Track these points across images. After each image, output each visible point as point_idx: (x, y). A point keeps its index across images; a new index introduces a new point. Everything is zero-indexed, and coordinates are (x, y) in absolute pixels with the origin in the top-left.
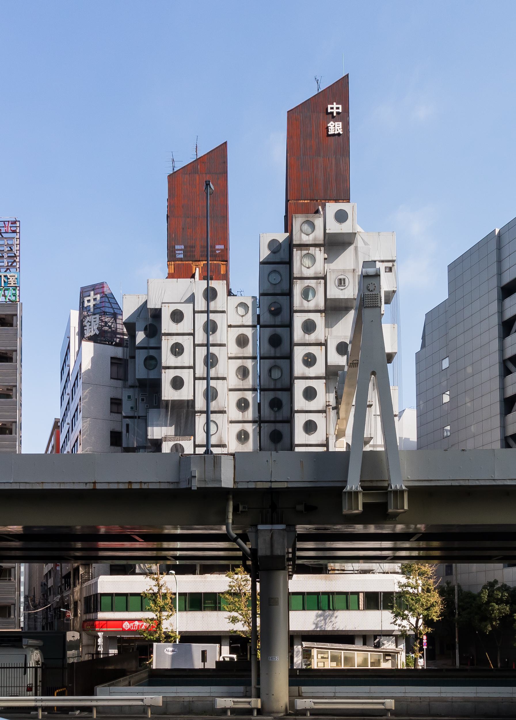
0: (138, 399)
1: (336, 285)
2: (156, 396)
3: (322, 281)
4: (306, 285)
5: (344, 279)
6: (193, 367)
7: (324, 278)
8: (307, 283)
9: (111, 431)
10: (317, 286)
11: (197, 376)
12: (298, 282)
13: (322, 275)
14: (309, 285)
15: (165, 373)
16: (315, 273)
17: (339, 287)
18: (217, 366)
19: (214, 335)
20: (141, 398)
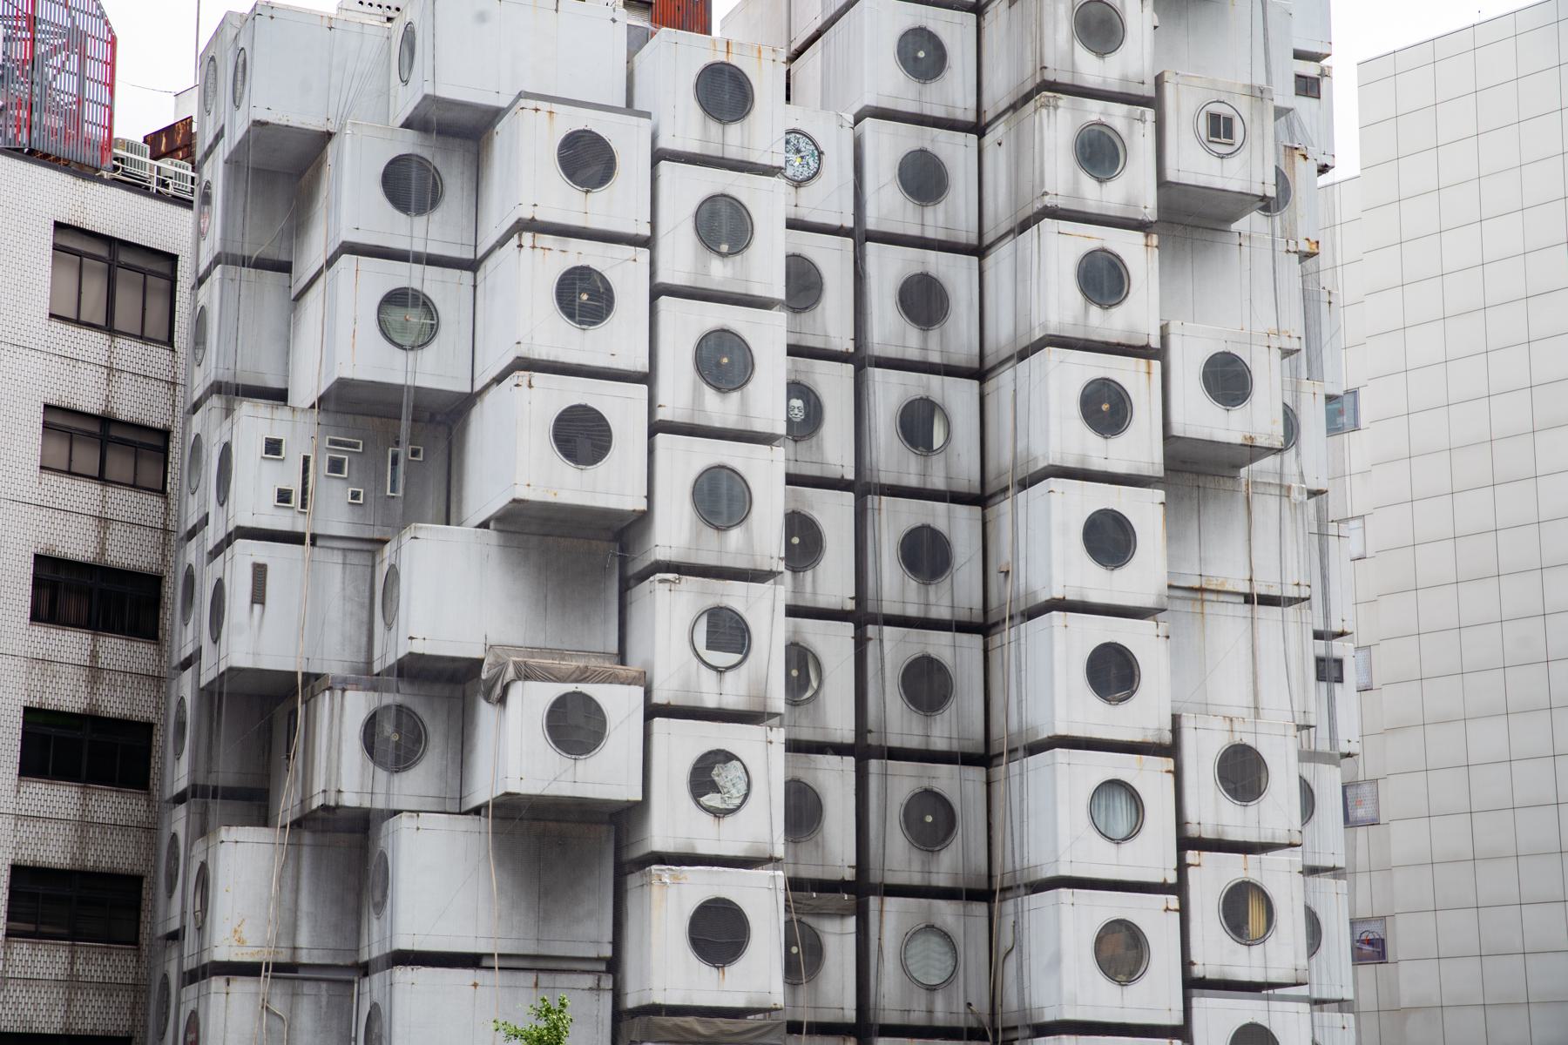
0: (316, 461)
1: (1201, 143)
2: (395, 462)
3: (1150, 114)
4: (1094, 118)
5: (1229, 121)
6: (647, 379)
7: (1154, 102)
8: (1094, 110)
9: (37, 556)
10: (1130, 127)
11: (662, 415)
12: (1060, 103)
13: (1148, 90)
14: (1103, 120)
15: (530, 386)
16: (1125, 79)
17: (1213, 146)
18: (750, 386)
19: (738, 258)
20: (330, 458)
